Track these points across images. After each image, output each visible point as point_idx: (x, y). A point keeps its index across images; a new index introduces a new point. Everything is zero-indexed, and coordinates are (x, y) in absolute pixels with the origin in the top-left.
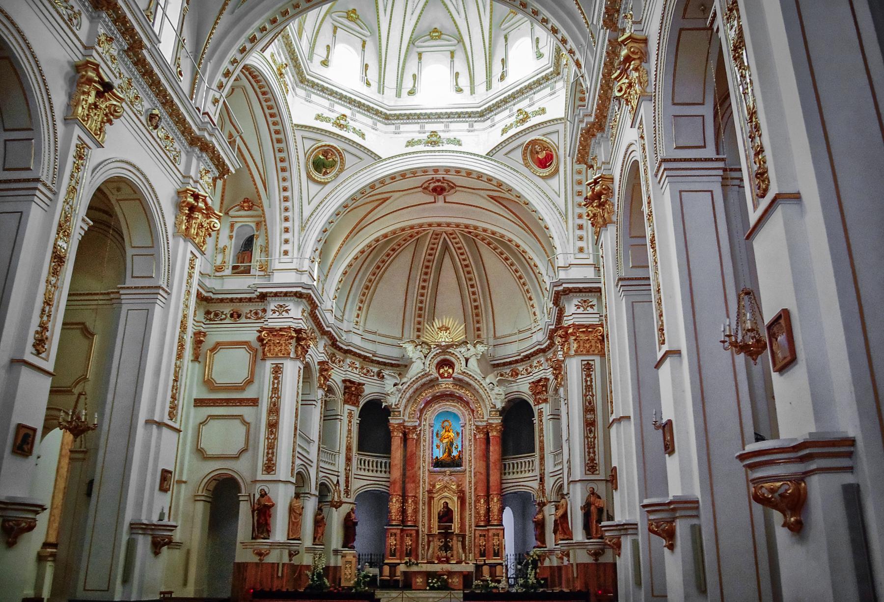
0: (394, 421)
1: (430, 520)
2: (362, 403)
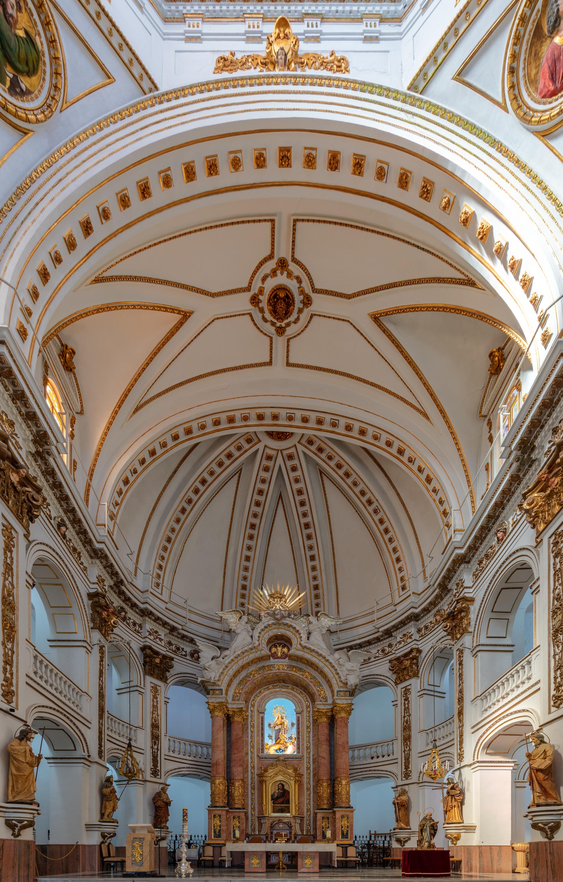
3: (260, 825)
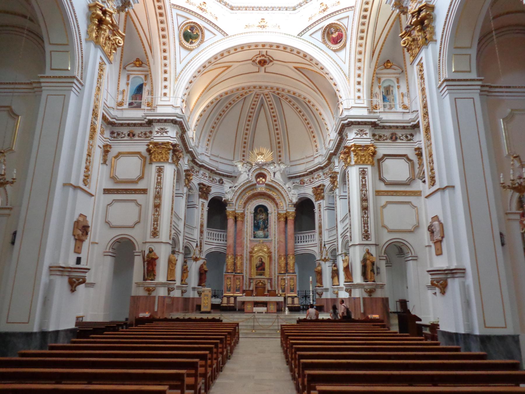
0: (229, 209)
1: (251, 269)
2: (210, 198)
3: (250, 283)
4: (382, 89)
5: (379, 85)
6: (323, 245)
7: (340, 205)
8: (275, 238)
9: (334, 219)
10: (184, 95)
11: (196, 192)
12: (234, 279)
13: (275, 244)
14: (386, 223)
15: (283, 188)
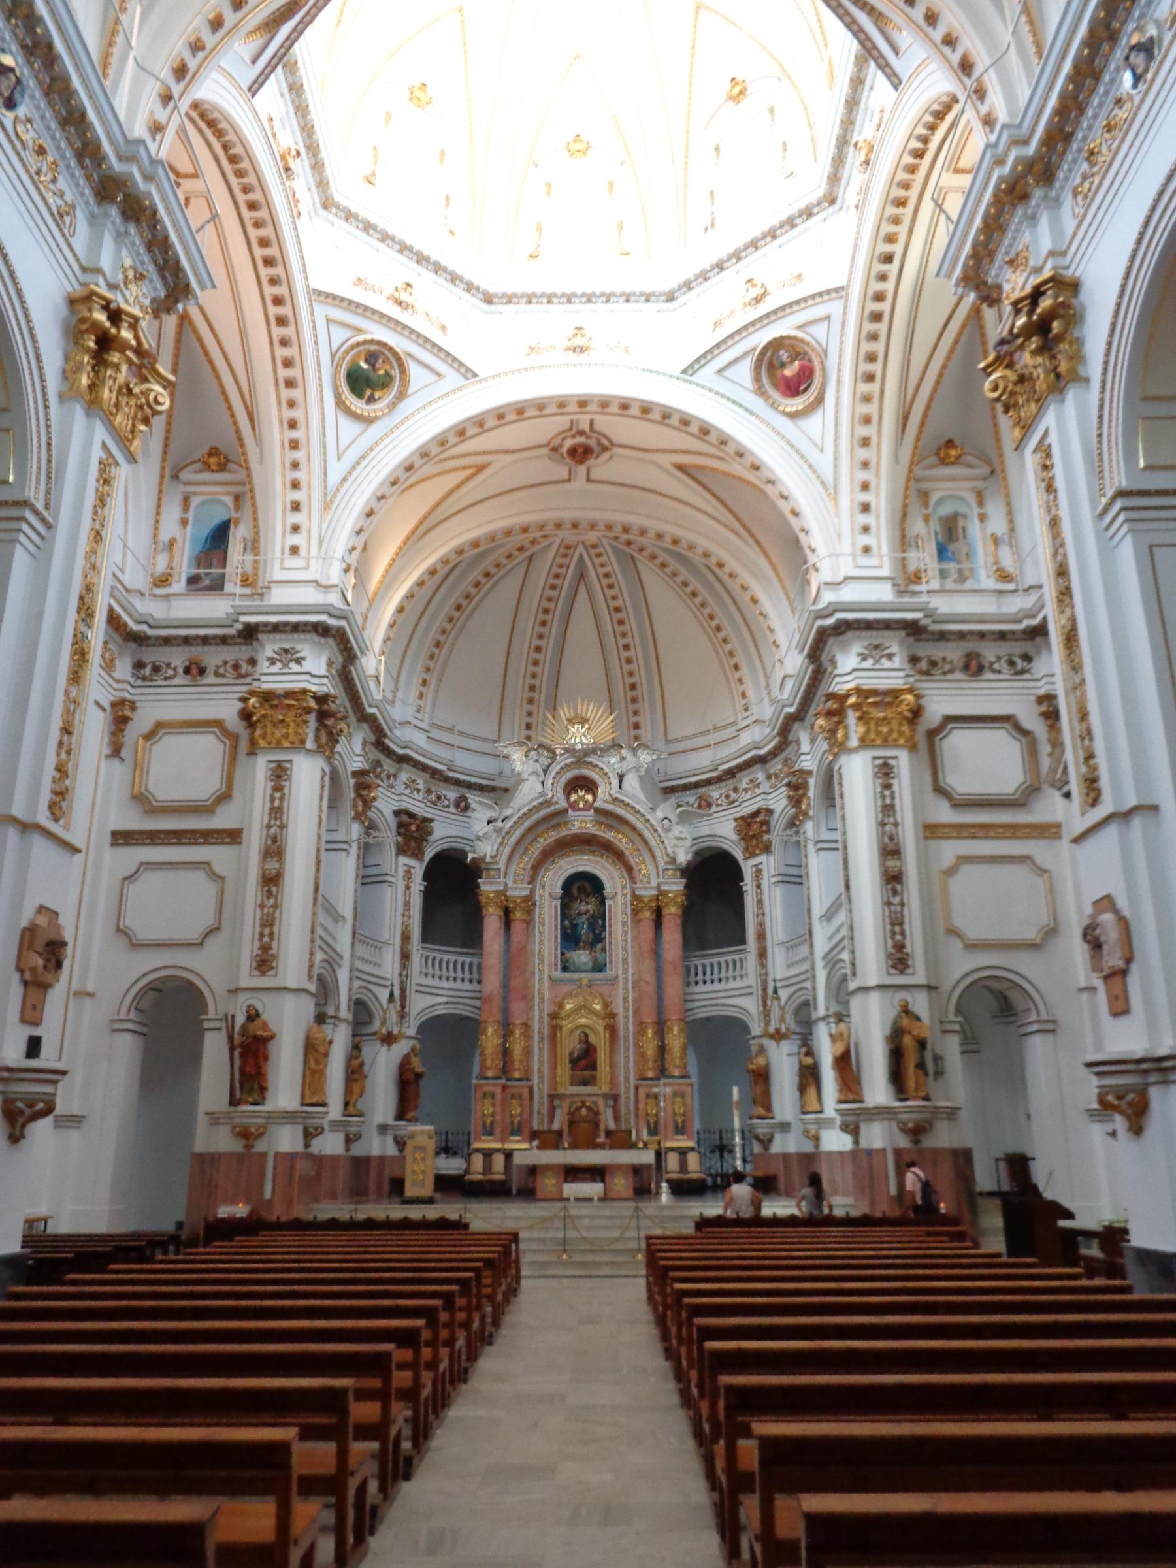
0: (487, 887)
1: (554, 1067)
2: (429, 853)
3: (552, 1110)
4: (935, 526)
5: (925, 511)
6: (770, 991)
7: (819, 867)
8: (625, 971)
9: (801, 912)
10: (350, 552)
11: (389, 836)
12: (503, 1098)
13: (626, 988)
14: (958, 922)
15: (648, 821)
